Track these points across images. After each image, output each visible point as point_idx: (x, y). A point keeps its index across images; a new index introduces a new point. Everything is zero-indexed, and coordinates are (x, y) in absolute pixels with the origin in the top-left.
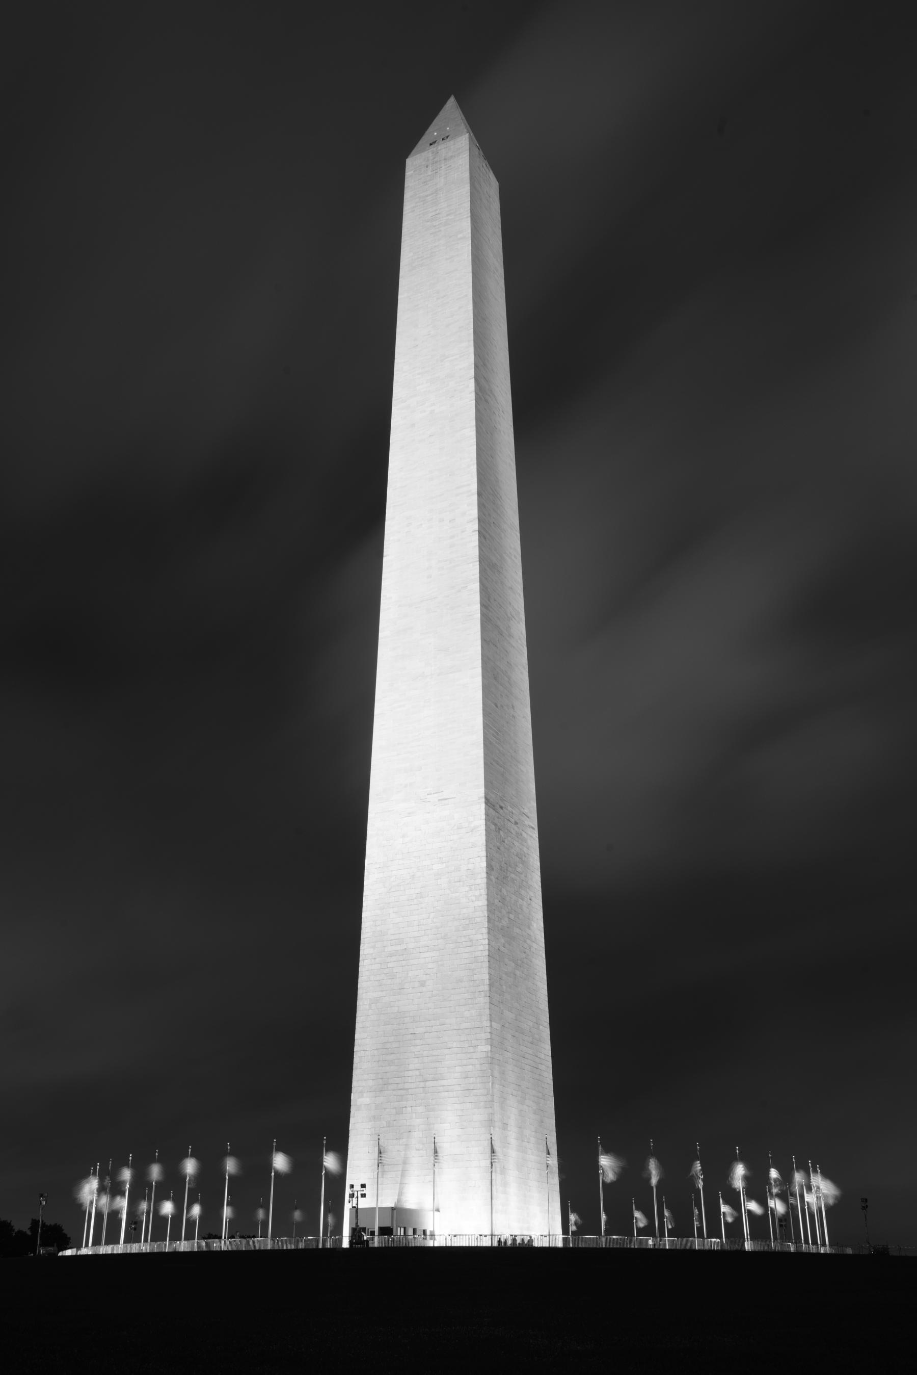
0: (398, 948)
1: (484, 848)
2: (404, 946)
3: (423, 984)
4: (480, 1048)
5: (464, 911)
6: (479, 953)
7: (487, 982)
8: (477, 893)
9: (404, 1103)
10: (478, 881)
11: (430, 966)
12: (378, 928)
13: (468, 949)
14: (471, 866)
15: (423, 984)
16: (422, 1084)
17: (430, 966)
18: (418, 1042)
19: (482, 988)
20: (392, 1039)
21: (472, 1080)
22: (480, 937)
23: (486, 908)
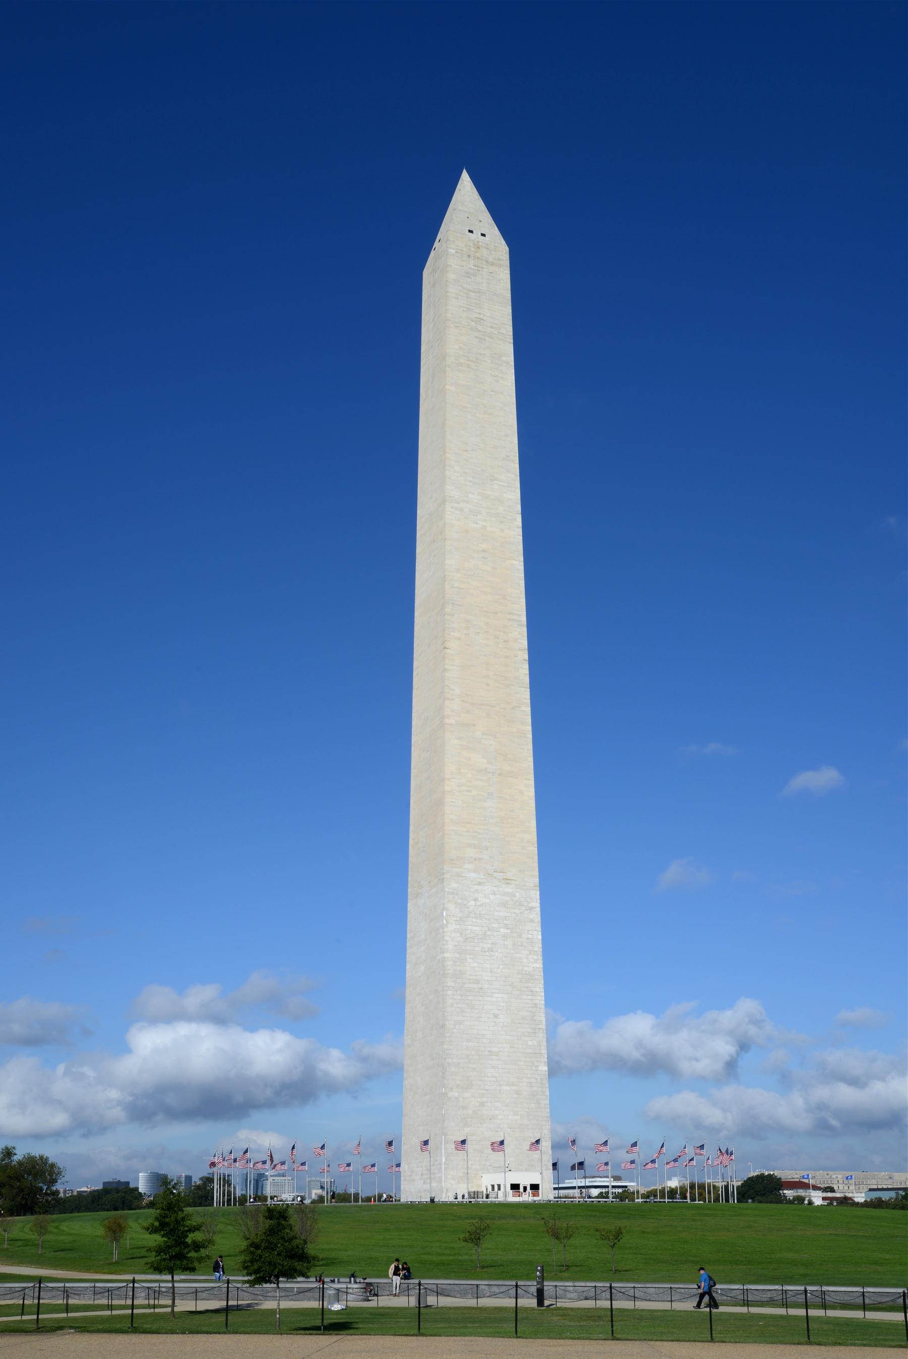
0: (475, 986)
1: (540, 925)
2: (480, 986)
3: (496, 1016)
4: (540, 1068)
5: (526, 968)
6: (538, 1002)
7: (544, 1023)
8: (535, 957)
9: (485, 1099)
10: (536, 949)
11: (502, 1004)
12: (458, 968)
13: (529, 997)
14: (530, 936)
15: (496, 1016)
16: (498, 1088)
17: (502, 1004)
18: (494, 1057)
19: (540, 1026)
20: (473, 1053)
21: (535, 1089)
22: (538, 990)
23: (542, 970)
